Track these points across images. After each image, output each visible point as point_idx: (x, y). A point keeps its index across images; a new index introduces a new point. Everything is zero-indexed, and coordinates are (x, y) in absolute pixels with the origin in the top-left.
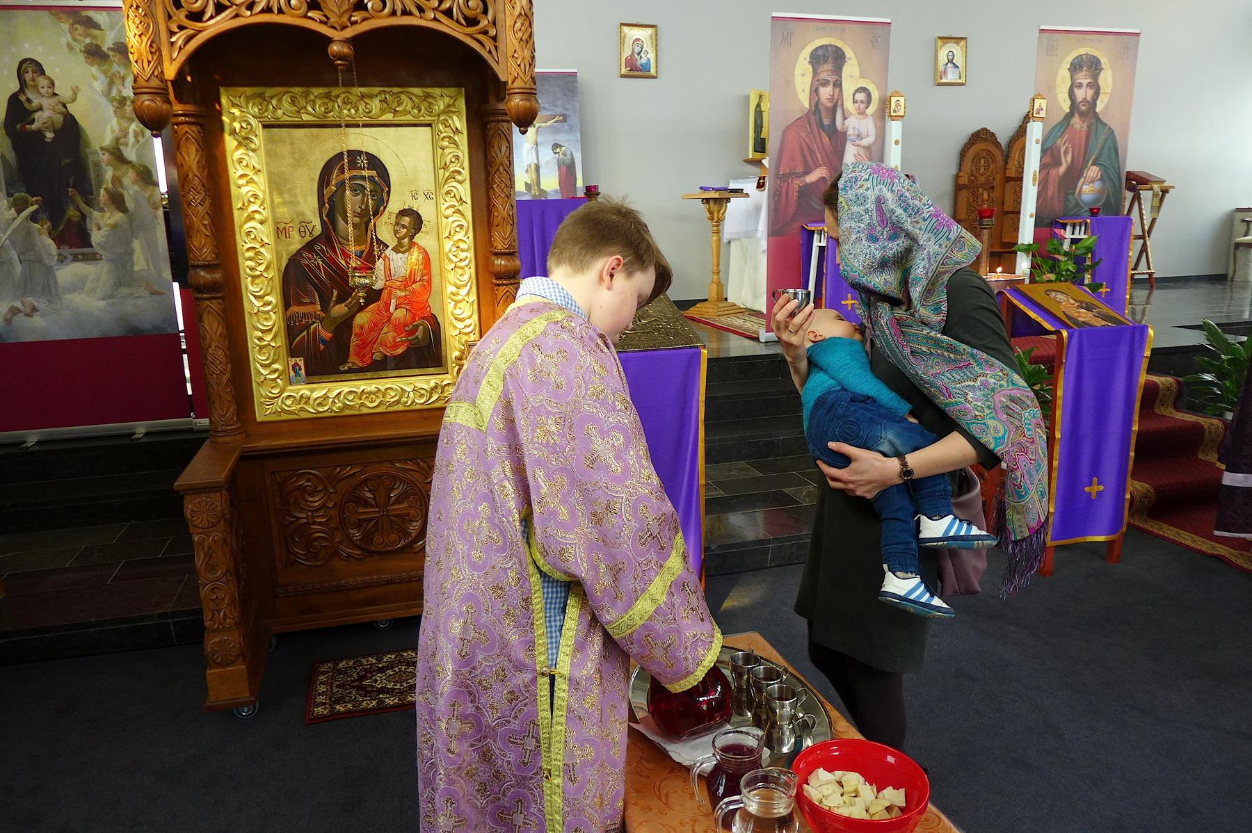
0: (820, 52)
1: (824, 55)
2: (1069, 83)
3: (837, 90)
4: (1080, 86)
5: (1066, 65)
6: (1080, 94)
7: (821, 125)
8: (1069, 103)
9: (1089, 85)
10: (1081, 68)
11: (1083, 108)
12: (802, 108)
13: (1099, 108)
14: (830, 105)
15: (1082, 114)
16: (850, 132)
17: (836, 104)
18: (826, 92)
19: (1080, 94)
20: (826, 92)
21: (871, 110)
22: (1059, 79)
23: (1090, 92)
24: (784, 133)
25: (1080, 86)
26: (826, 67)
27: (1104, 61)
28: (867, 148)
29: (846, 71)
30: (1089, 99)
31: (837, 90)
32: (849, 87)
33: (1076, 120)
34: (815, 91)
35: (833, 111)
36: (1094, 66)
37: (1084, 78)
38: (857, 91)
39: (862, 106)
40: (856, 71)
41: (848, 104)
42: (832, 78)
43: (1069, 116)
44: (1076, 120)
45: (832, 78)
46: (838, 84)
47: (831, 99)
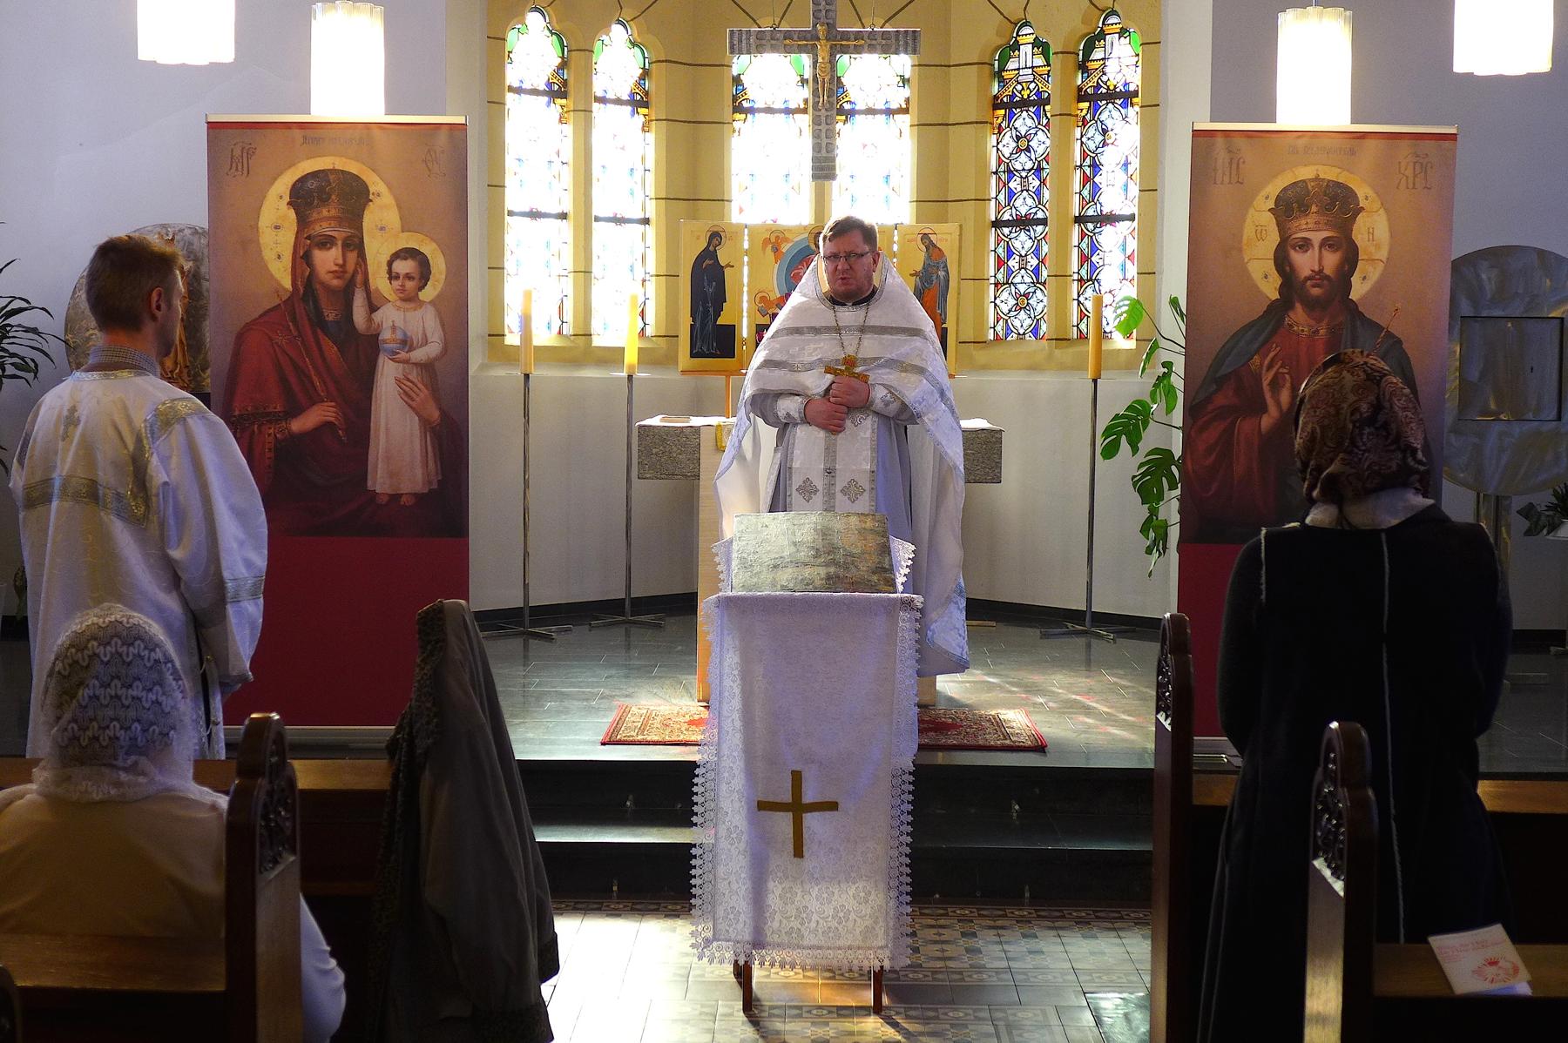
0: (312, 184)
1: (321, 190)
3: (352, 257)
7: (319, 322)
12: (278, 289)
14: (335, 282)
16: (386, 335)
17: (353, 279)
18: (327, 260)
20: (327, 260)
21: (428, 293)
24: (240, 337)
26: (325, 213)
28: (427, 367)
29: (370, 219)
31: (352, 257)
32: (378, 250)
34: (302, 258)
35: (345, 296)
38: (397, 256)
39: (410, 285)
40: (392, 218)
41: (380, 282)
42: (340, 234)
45: (340, 234)
46: (355, 244)
47: (341, 271)
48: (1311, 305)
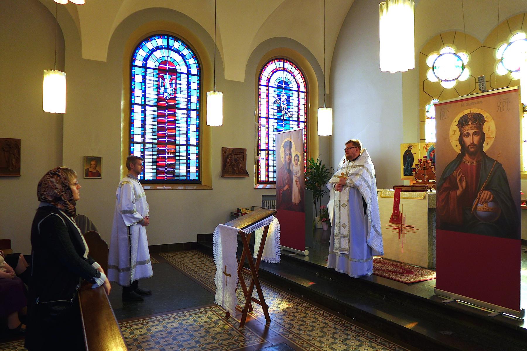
2: (458, 134)
4: (468, 135)
5: (455, 123)
6: (468, 141)
8: (460, 147)
9: (474, 134)
10: (467, 123)
11: (472, 150)
13: (486, 148)
15: (471, 154)
19: (468, 141)
23: (476, 139)
25: (468, 135)
30: (476, 143)
33: (467, 158)
36: (478, 120)
37: (470, 129)
44: (467, 158)
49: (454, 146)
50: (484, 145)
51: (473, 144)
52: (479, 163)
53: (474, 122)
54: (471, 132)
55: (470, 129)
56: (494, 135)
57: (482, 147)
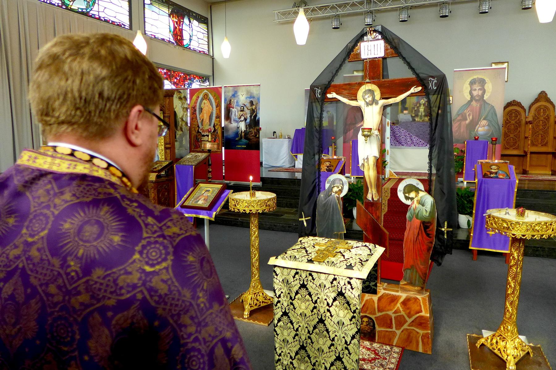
4: (475, 90)
6: (475, 93)
10: (475, 83)
22: (464, 88)
23: (480, 93)
25: (475, 90)
27: (487, 80)
33: (474, 103)
36: (482, 82)
37: (477, 87)
43: (471, 101)
44: (474, 103)
48: (476, 101)
49: (466, 96)
50: (485, 96)
51: (478, 95)
52: (481, 106)
53: (479, 83)
54: (477, 88)
55: (477, 87)
56: (491, 91)
57: (483, 97)
